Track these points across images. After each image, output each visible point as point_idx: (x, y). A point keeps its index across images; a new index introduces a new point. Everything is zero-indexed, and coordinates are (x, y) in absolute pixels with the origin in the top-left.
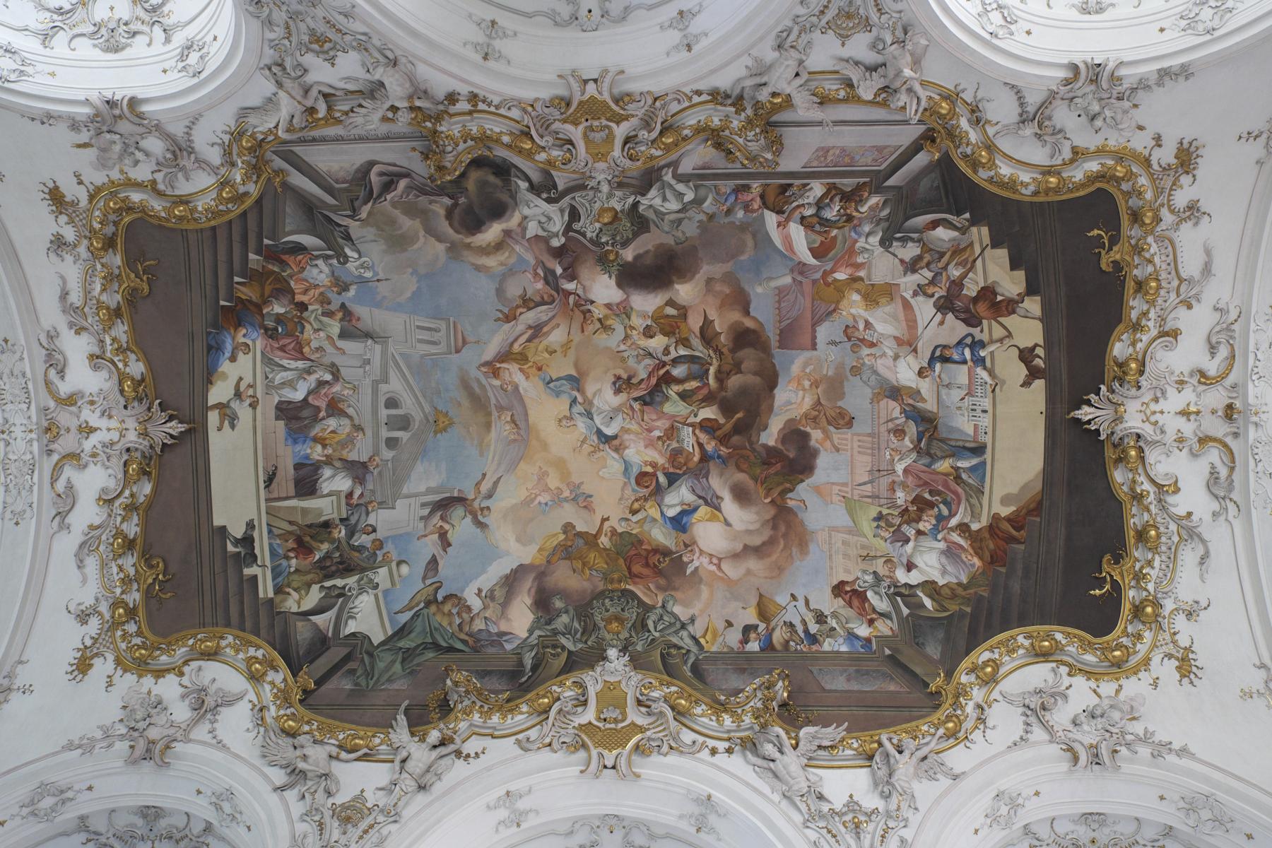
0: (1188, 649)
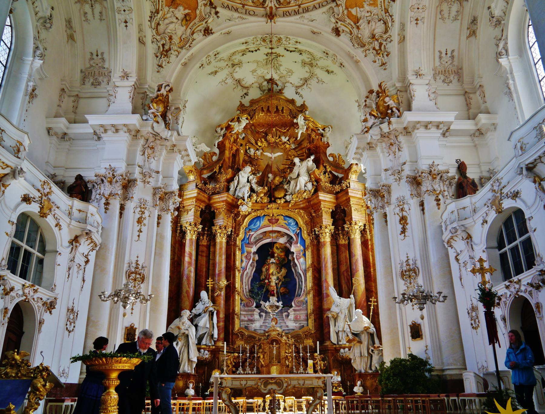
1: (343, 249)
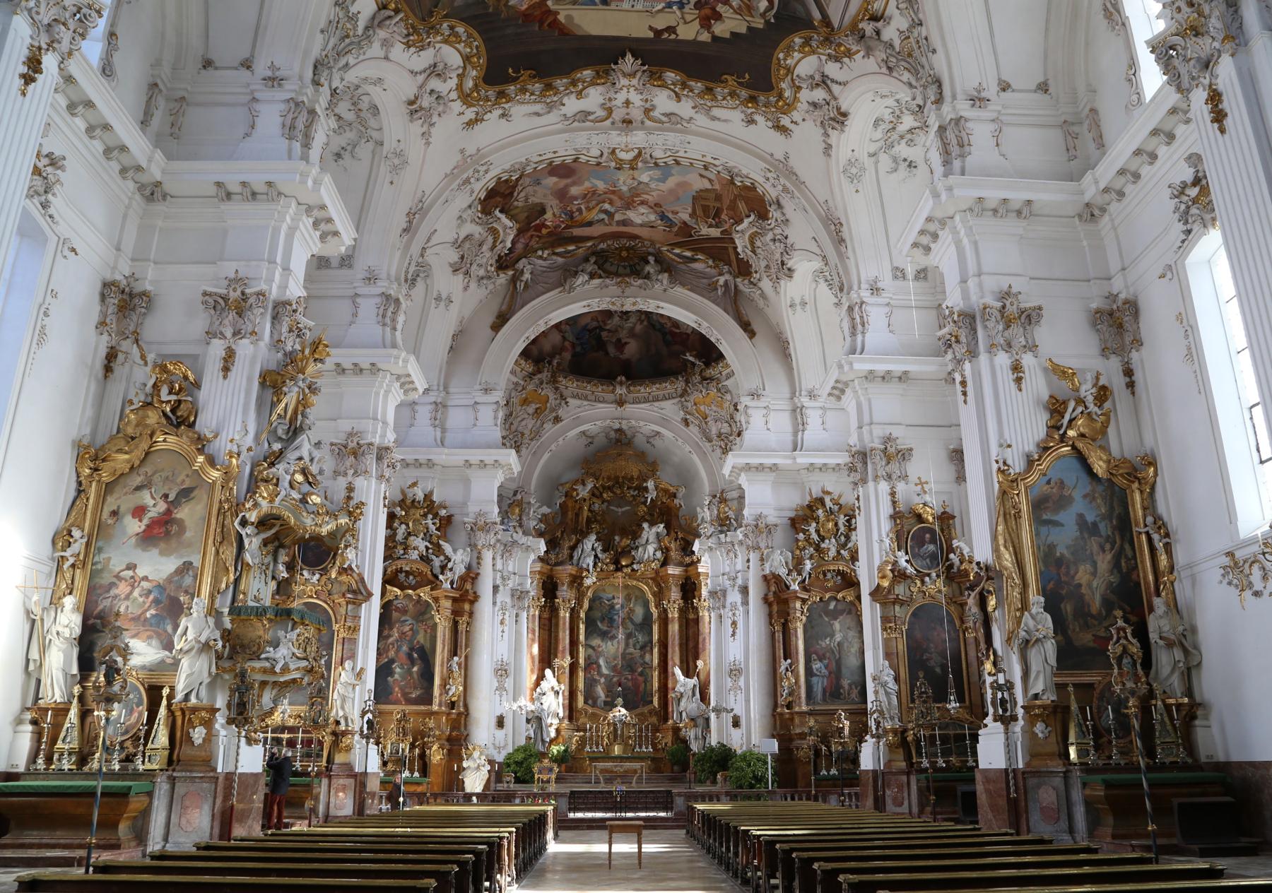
0: (483, 120)
1: (692, 624)
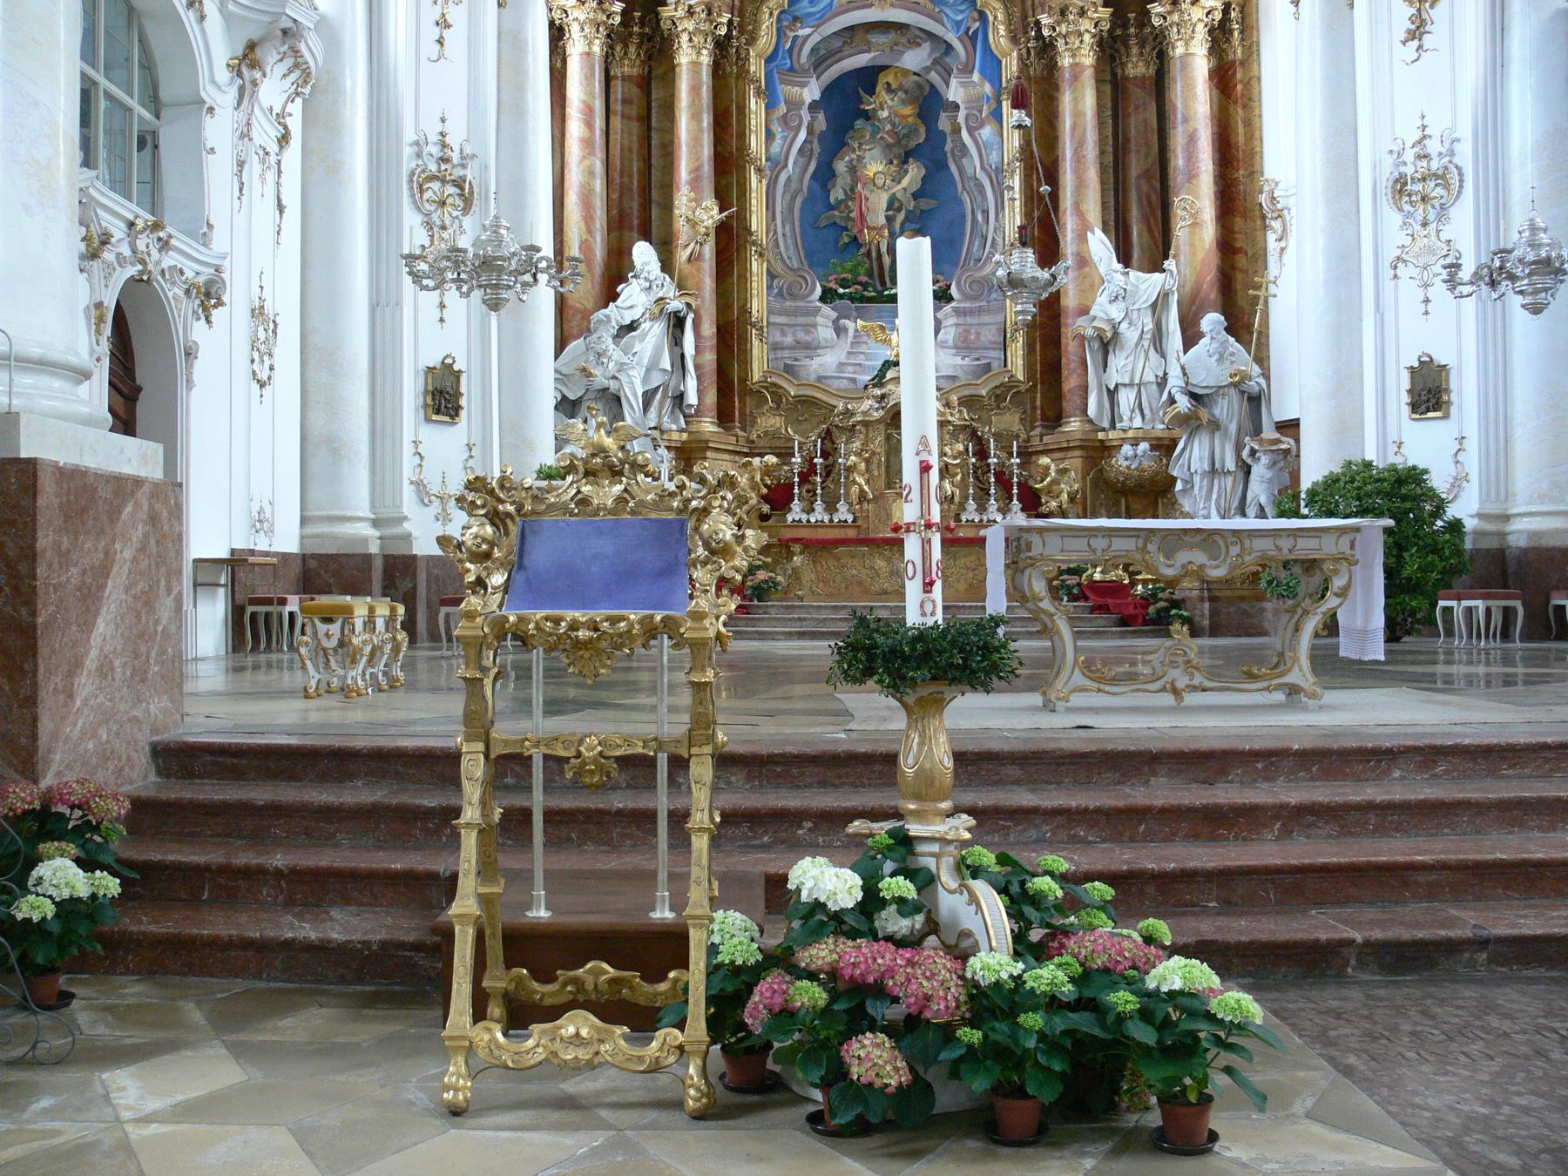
1: (1137, 94)
